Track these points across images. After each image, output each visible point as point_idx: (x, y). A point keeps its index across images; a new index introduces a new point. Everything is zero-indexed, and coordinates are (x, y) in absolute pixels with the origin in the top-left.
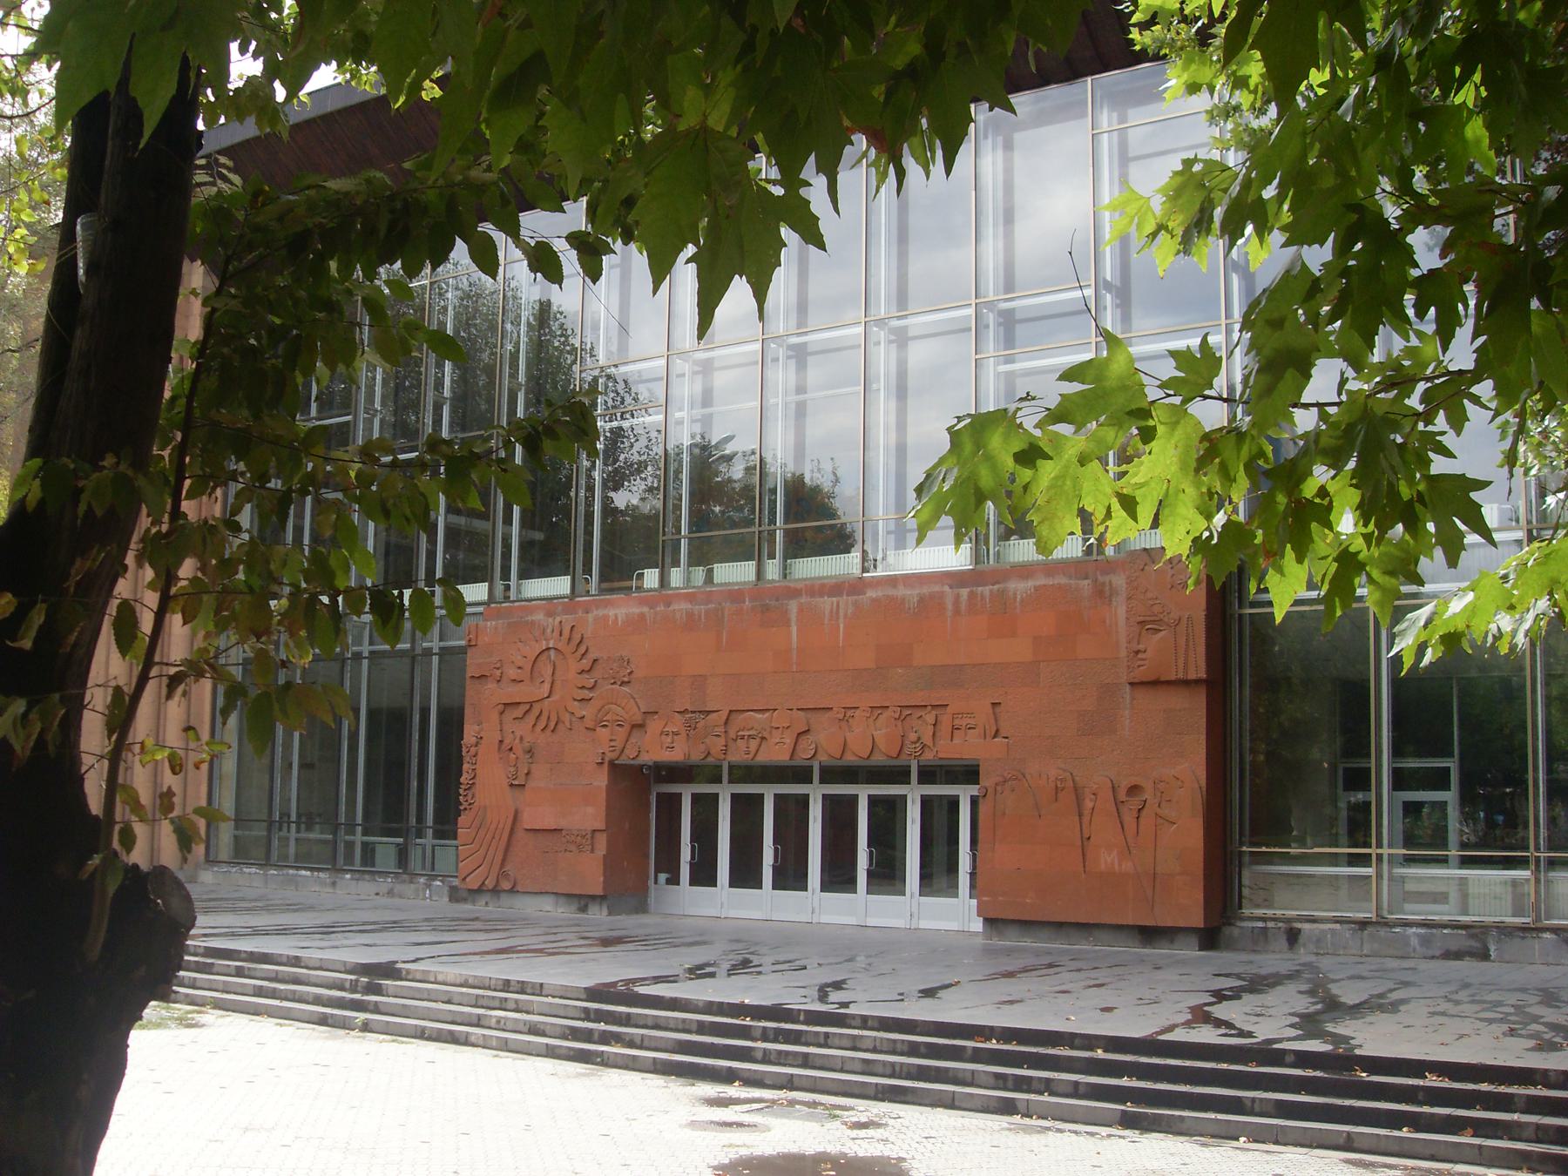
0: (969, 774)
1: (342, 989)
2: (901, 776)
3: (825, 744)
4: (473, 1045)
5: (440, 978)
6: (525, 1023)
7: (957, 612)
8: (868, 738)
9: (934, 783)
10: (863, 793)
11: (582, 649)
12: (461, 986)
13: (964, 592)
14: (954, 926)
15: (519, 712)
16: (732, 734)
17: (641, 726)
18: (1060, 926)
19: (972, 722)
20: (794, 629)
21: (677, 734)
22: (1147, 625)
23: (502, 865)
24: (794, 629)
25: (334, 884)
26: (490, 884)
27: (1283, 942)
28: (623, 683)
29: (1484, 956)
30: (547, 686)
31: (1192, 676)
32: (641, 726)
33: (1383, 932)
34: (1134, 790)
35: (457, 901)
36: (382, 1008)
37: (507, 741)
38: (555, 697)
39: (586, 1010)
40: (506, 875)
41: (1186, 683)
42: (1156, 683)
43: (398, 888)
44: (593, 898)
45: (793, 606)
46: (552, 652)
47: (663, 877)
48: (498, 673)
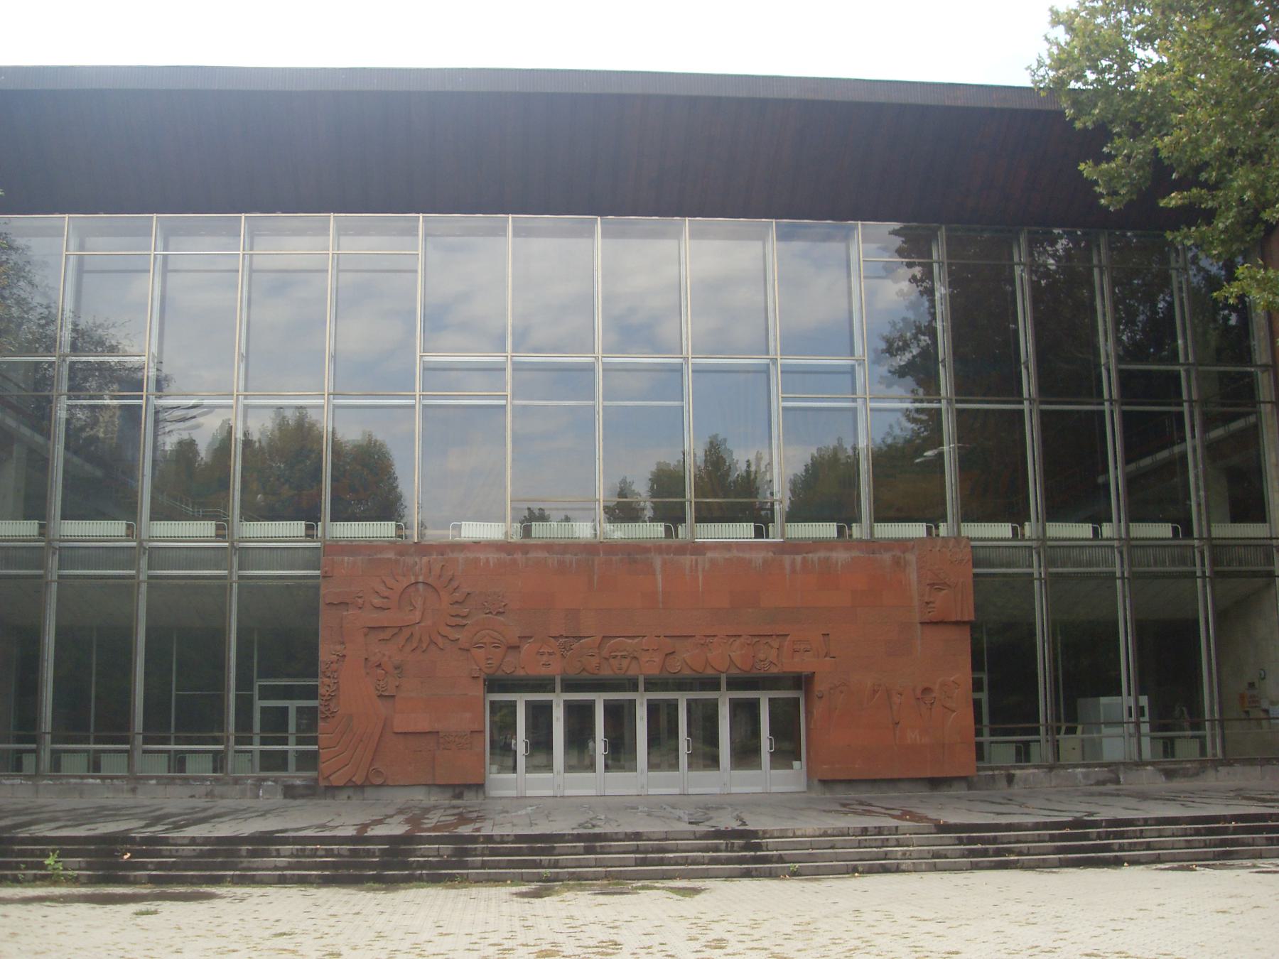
0: (802, 682)
1: (717, 849)
2: (713, 684)
3: (687, 660)
4: (904, 871)
5: (798, 833)
6: (929, 851)
7: (793, 571)
8: (727, 656)
9: (667, 690)
10: (682, 699)
11: (455, 584)
12: (820, 836)
13: (799, 558)
14: (759, 789)
15: (382, 635)
16: (605, 652)
17: (516, 648)
18: (874, 782)
19: (808, 647)
20: (659, 577)
21: (550, 654)
22: (936, 586)
23: (371, 765)
24: (659, 577)
25: (134, 790)
26: (358, 779)
27: (1004, 783)
28: (499, 613)
29: (1117, 782)
30: (417, 616)
31: (966, 619)
32: (516, 648)
33: (1062, 772)
34: (926, 690)
35: (294, 797)
36: (786, 858)
39: (959, 838)
40: (378, 773)
41: (957, 623)
42: (931, 623)
43: (218, 790)
44: (469, 787)
45: (658, 561)
46: (421, 587)
47: (495, 768)
48: (360, 601)
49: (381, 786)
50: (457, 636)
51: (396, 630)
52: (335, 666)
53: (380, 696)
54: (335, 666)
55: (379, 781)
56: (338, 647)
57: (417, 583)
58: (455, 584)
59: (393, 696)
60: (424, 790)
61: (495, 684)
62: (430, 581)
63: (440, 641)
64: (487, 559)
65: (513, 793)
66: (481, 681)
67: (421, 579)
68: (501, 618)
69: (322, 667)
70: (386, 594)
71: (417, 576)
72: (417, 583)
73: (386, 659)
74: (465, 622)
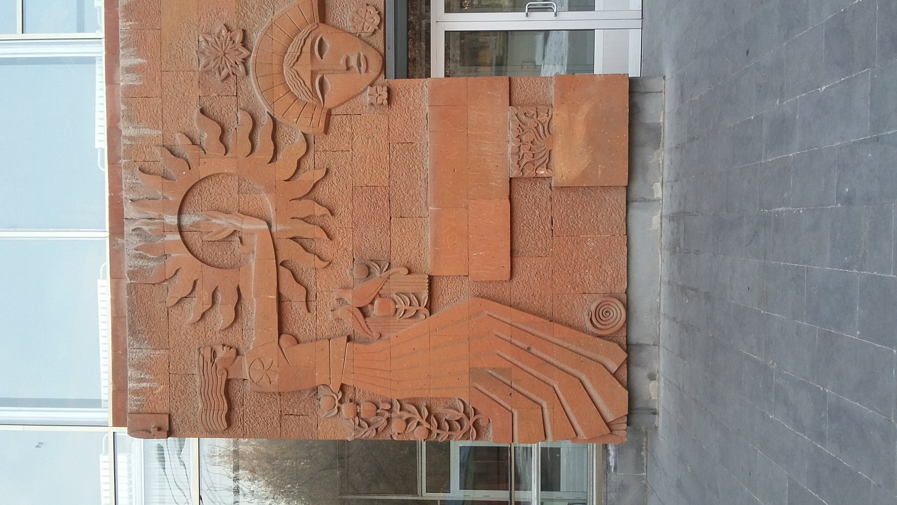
11: (180, 142)
15: (295, 307)
26: (614, 359)
28: (244, 43)
37: (350, 324)
38: (272, 216)
44: (634, 111)
46: (187, 220)
48: (221, 353)
49: (627, 307)
50: (299, 139)
51: (285, 273)
52: (365, 409)
53: (430, 308)
54: (365, 409)
55: (618, 313)
56: (324, 402)
57: (180, 229)
58: (180, 142)
59: (431, 279)
60: (637, 214)
61: (414, 63)
62: (175, 199)
63: (308, 176)
64: (129, 70)
65: (635, 38)
66: (400, 84)
67: (171, 220)
68: (255, 39)
69: (370, 434)
70: (207, 298)
71: (165, 229)
72: (180, 229)
73: (348, 297)
74: (265, 121)
